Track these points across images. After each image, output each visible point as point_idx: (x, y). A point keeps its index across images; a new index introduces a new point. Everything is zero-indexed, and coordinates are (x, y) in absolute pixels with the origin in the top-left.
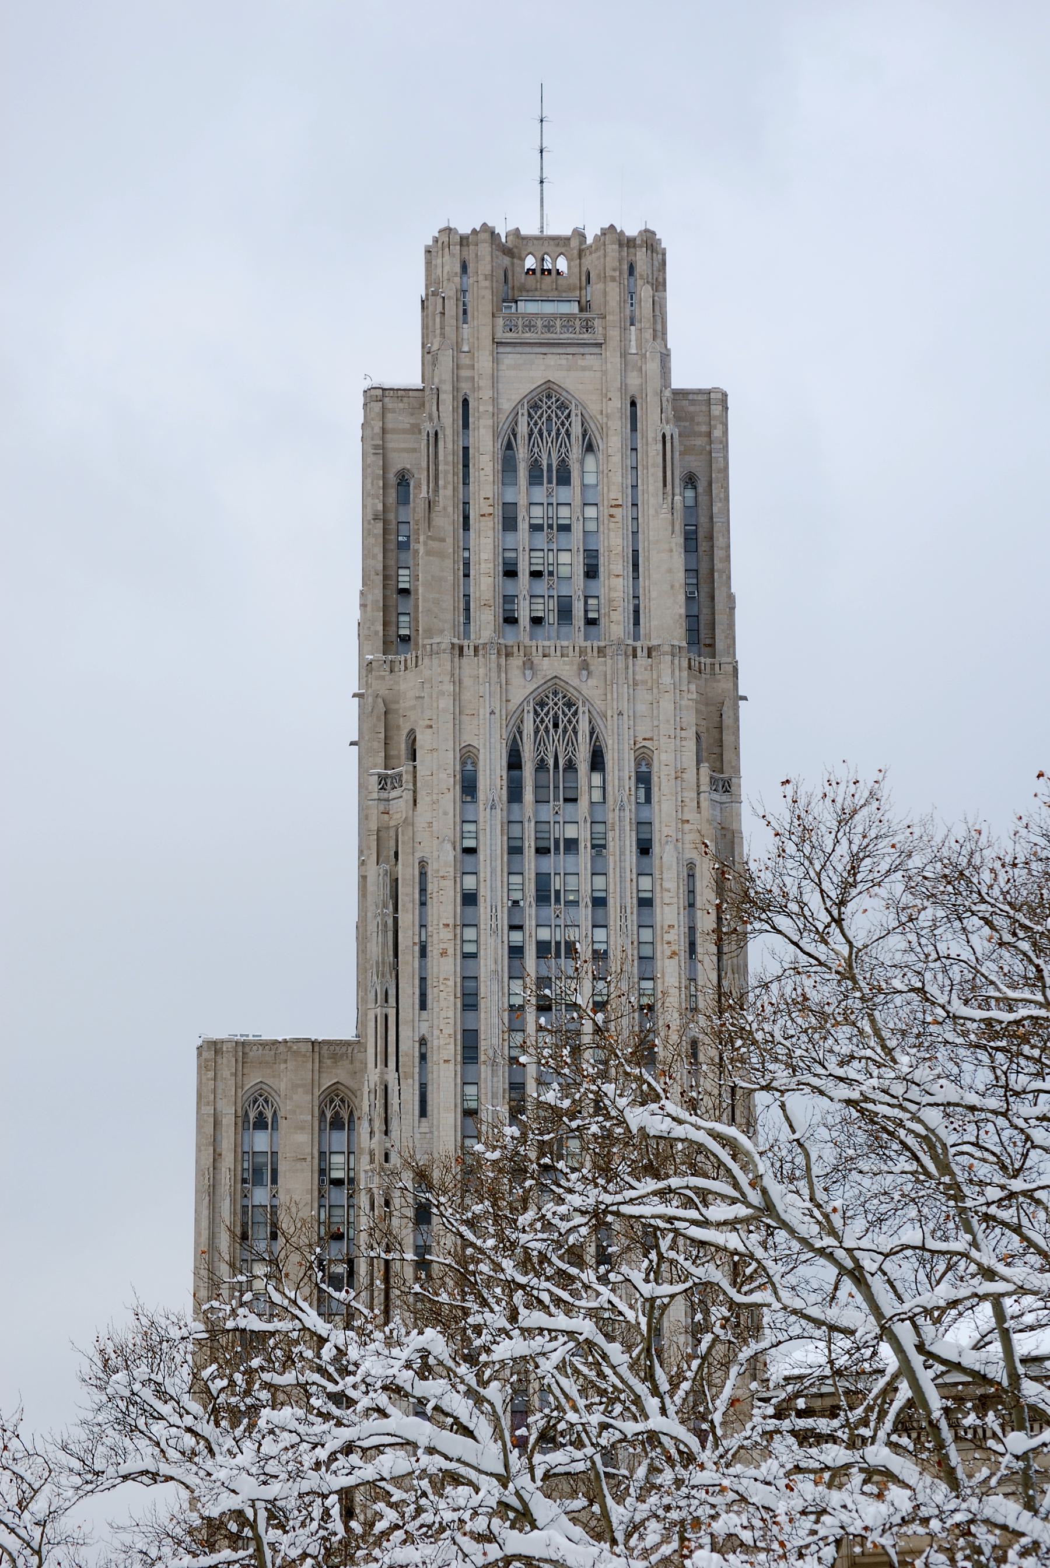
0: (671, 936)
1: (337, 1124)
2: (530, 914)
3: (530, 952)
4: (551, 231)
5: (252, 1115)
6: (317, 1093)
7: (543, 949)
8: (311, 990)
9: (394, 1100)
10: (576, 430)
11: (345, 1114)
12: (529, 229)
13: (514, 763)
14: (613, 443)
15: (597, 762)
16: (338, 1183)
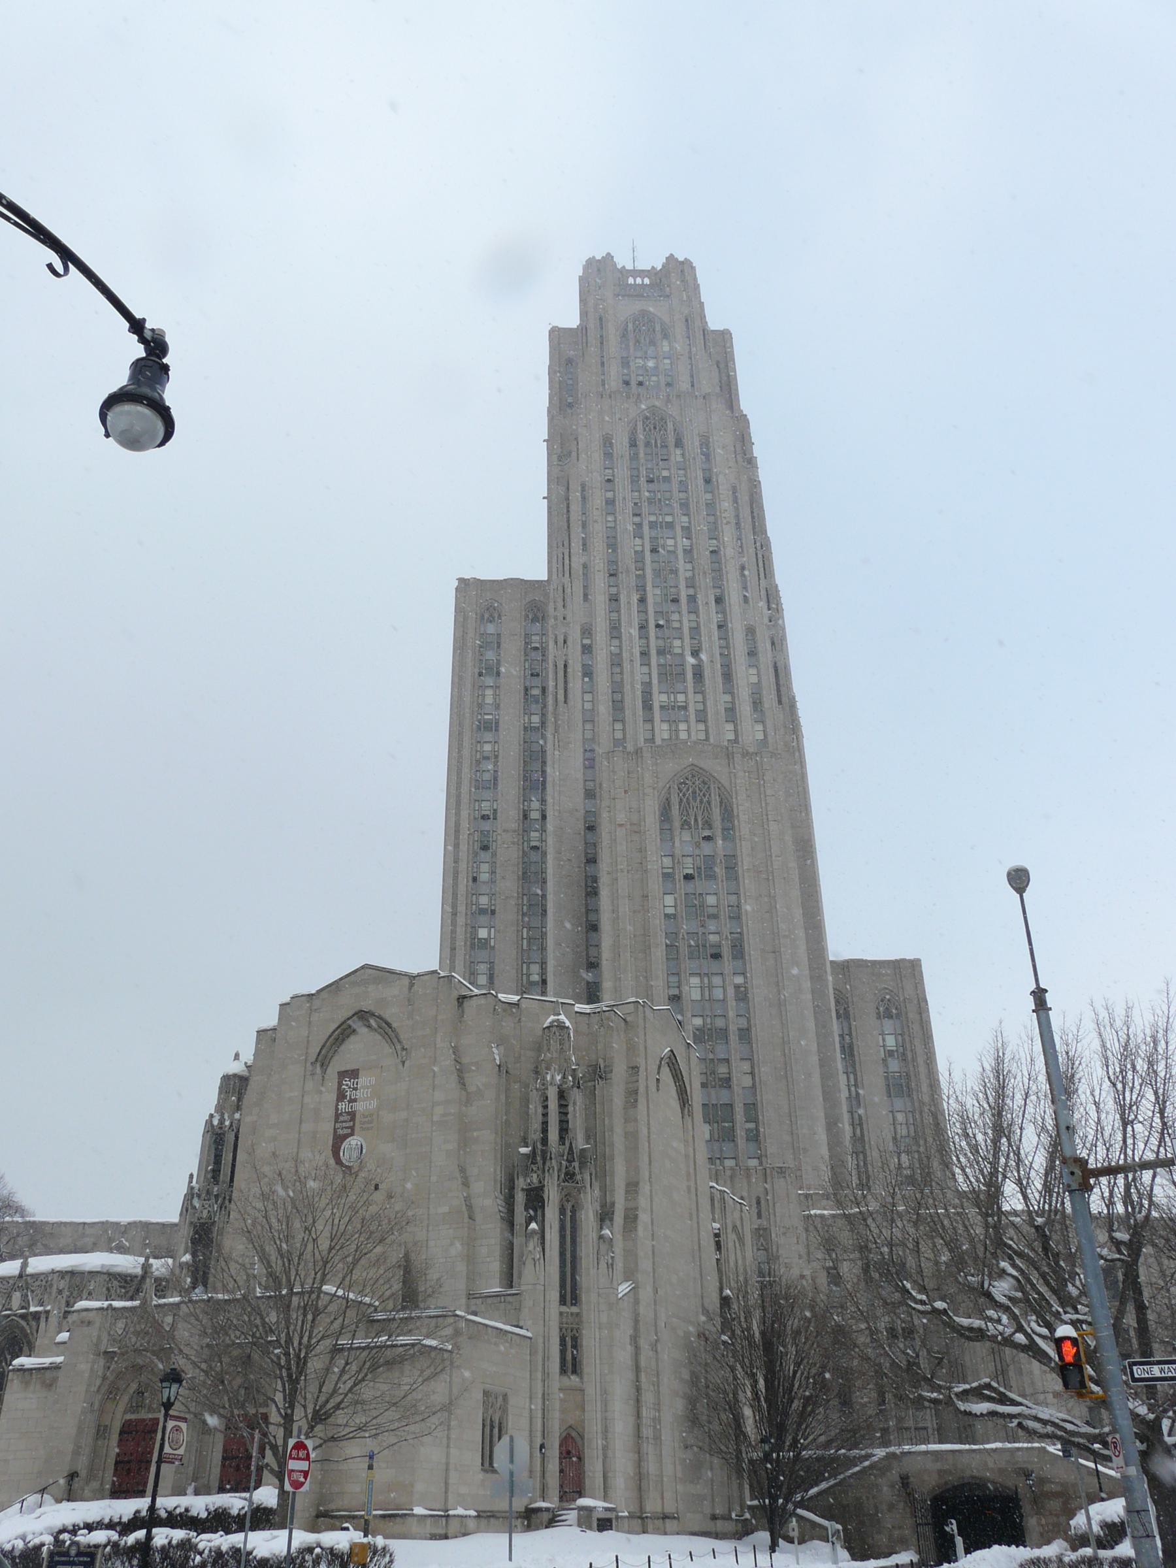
0: (726, 515)
1: (535, 620)
2: (645, 509)
3: (646, 528)
4: (640, 267)
5: (486, 616)
6: (524, 602)
7: (652, 525)
8: (521, 552)
9: (568, 591)
10: (658, 328)
11: (540, 615)
12: (629, 267)
13: (633, 444)
14: (679, 330)
15: (679, 443)
16: (536, 649)
